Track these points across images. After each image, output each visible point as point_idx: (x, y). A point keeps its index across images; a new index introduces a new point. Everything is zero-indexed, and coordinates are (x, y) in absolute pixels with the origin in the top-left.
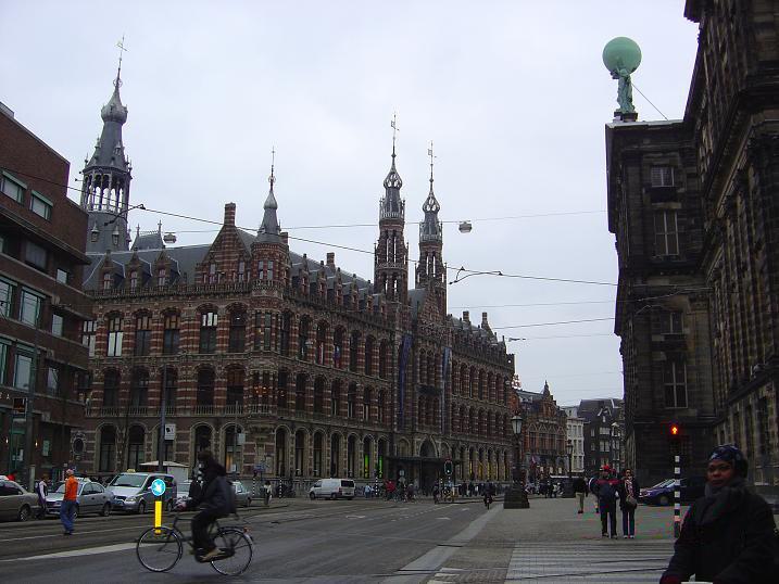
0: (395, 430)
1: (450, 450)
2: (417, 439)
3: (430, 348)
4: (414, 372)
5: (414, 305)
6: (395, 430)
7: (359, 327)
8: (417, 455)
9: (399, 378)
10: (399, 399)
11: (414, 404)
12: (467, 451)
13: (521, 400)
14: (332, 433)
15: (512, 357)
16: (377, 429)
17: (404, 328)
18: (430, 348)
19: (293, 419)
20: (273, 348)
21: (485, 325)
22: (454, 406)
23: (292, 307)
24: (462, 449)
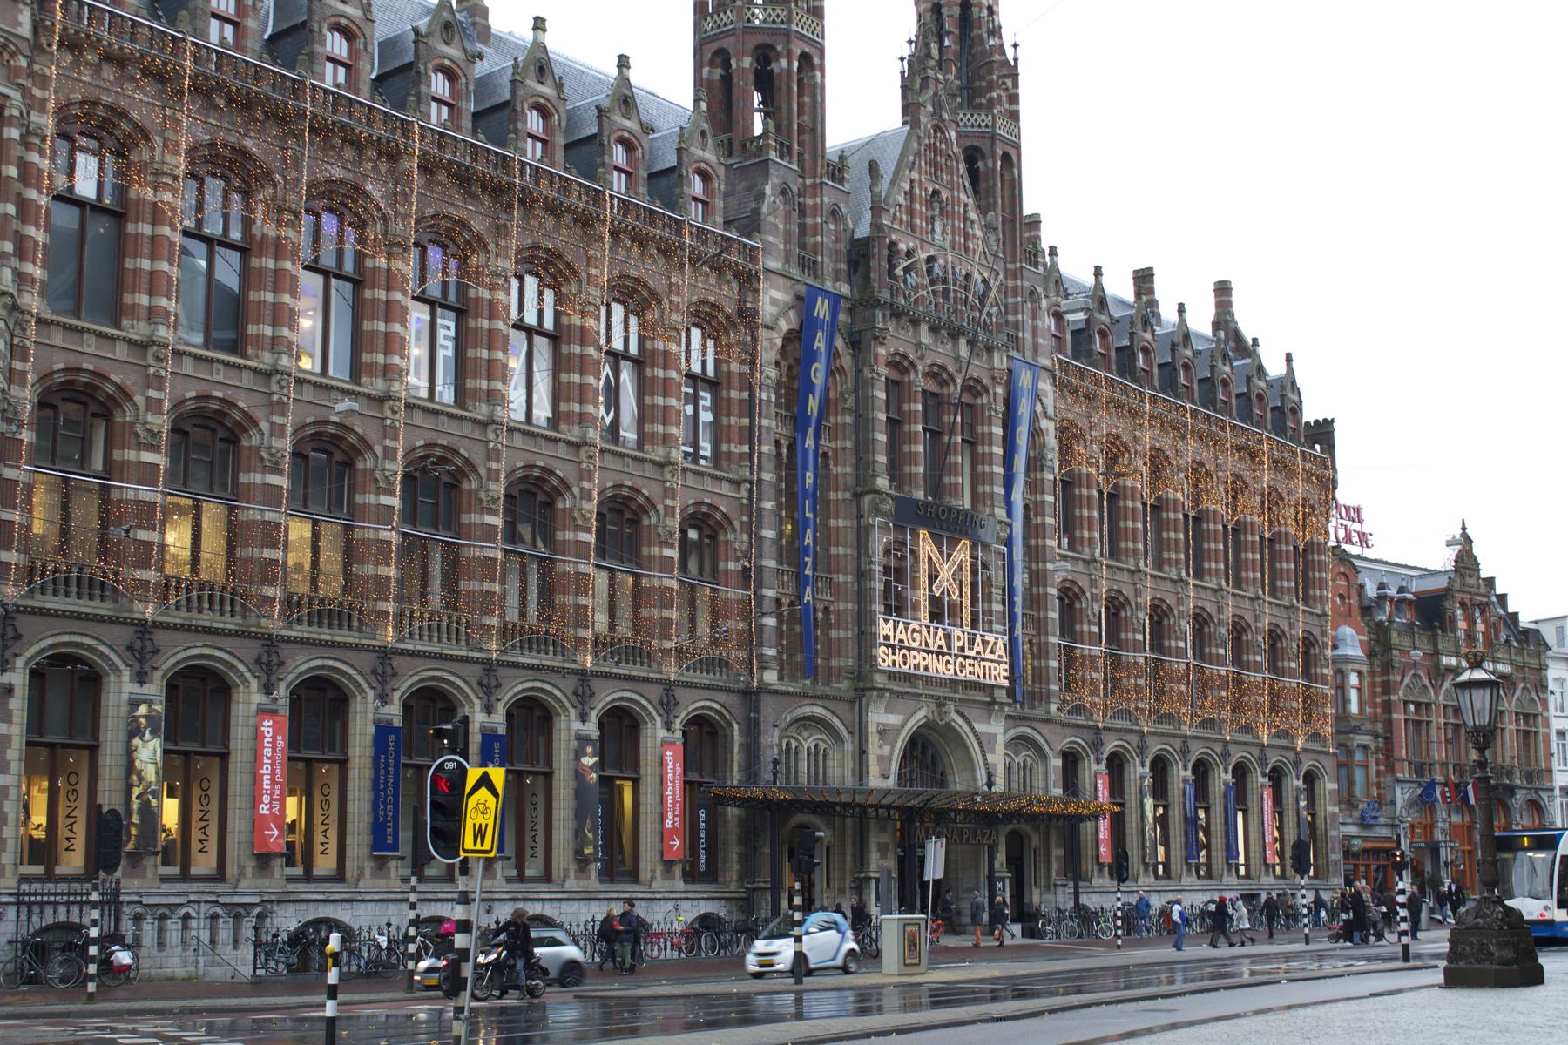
0: (771, 677)
1: (1056, 762)
2: (879, 716)
3: (940, 352)
4: (863, 447)
5: (857, 174)
6: (771, 677)
7: (562, 239)
8: (883, 776)
9: (790, 464)
10: (791, 552)
11: (862, 575)
12: (1139, 772)
13: (1371, 591)
14: (405, 685)
15: (1323, 432)
16: (672, 672)
17: (809, 266)
18: (940, 352)
21: (1224, 319)
22: (1070, 597)
23: (140, 102)
24: (1116, 764)
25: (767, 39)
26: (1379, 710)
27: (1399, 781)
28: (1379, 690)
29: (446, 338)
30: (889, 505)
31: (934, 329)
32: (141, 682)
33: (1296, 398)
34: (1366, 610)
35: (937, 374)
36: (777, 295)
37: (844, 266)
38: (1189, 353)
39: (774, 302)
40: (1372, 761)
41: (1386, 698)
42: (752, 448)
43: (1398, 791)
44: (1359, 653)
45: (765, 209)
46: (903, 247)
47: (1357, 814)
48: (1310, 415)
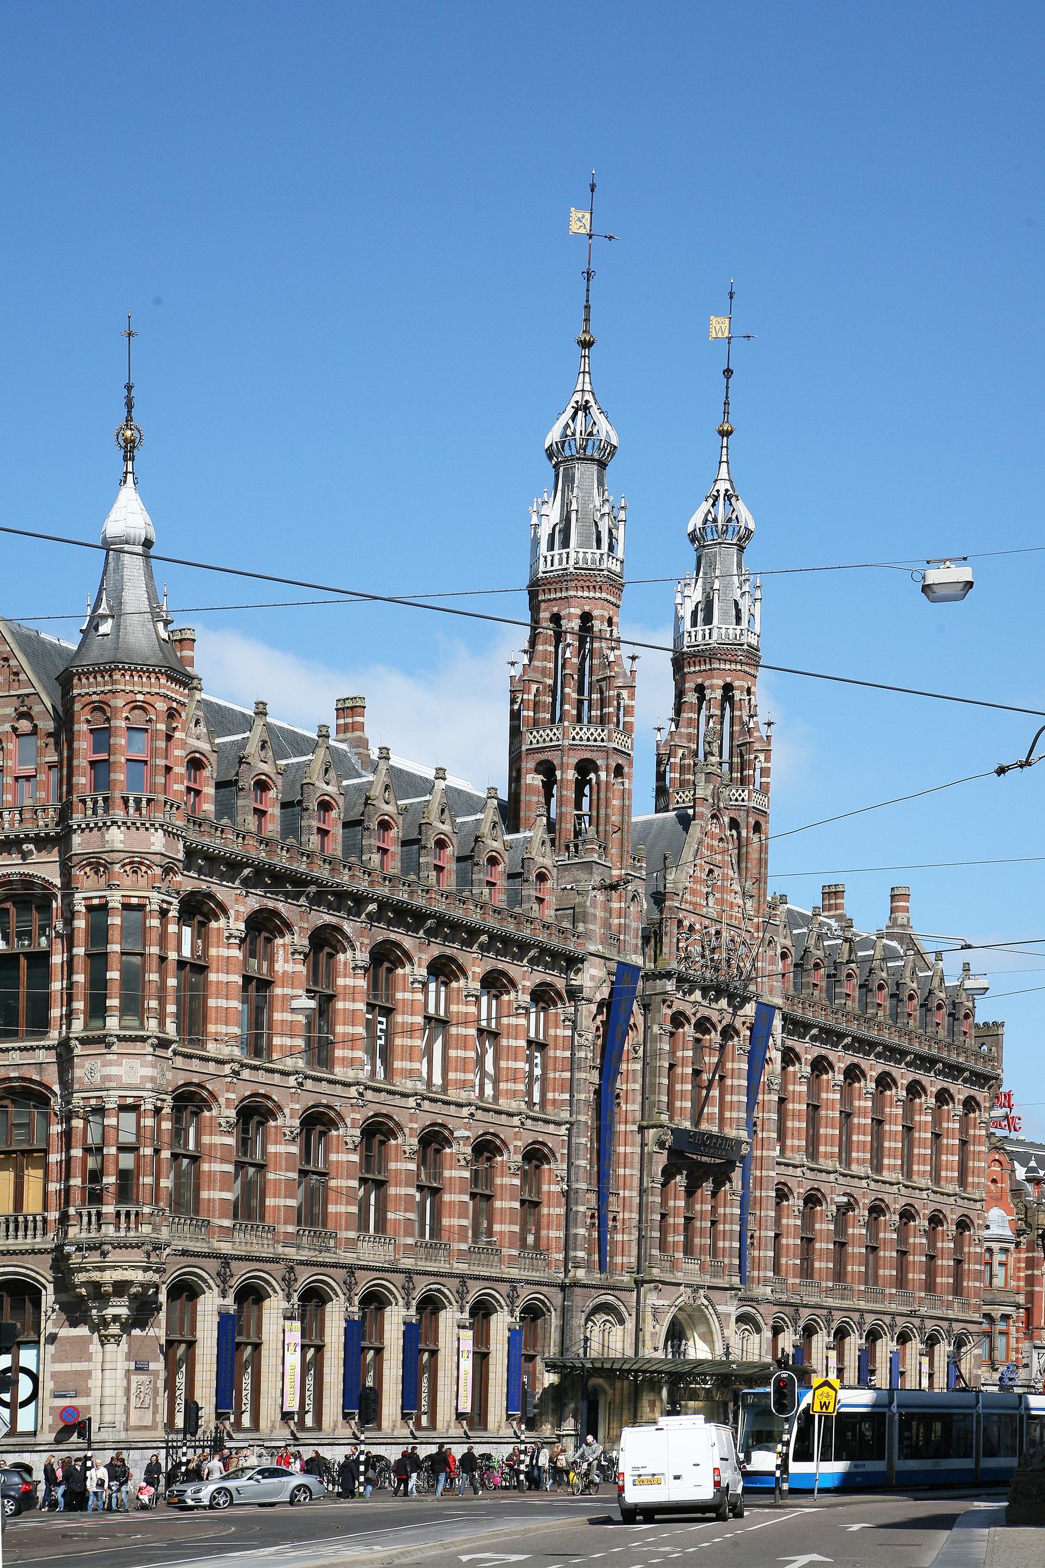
15: (991, 1032)
19: (225, 1248)
20: (152, 1024)
25: (587, 755)
26: (1022, 1284)
27: (1036, 1347)
28: (1023, 1265)
29: (381, 1030)
30: (669, 1139)
31: (705, 991)
32: (224, 1297)
33: (970, 1004)
34: (1017, 1192)
35: (703, 1025)
36: (594, 972)
37: (640, 942)
38: (884, 975)
39: (592, 978)
40: (1013, 1330)
41: (1029, 1272)
42: (572, 1096)
43: (1035, 1356)
44: (1008, 1233)
45: (588, 903)
46: (686, 923)
47: (996, 1376)
48: (980, 1019)
